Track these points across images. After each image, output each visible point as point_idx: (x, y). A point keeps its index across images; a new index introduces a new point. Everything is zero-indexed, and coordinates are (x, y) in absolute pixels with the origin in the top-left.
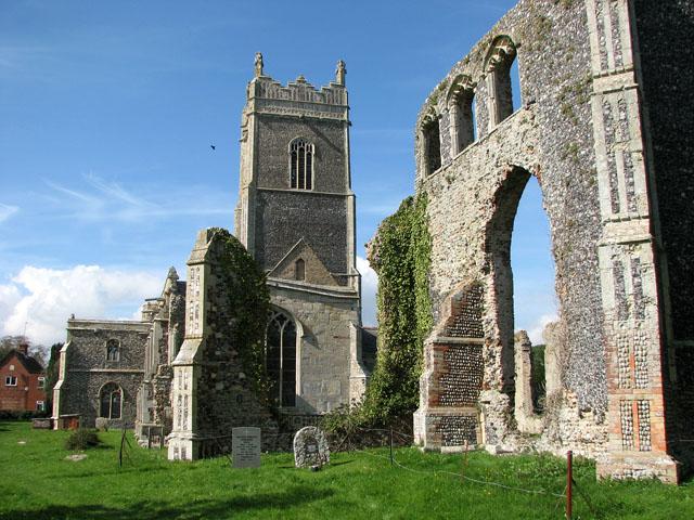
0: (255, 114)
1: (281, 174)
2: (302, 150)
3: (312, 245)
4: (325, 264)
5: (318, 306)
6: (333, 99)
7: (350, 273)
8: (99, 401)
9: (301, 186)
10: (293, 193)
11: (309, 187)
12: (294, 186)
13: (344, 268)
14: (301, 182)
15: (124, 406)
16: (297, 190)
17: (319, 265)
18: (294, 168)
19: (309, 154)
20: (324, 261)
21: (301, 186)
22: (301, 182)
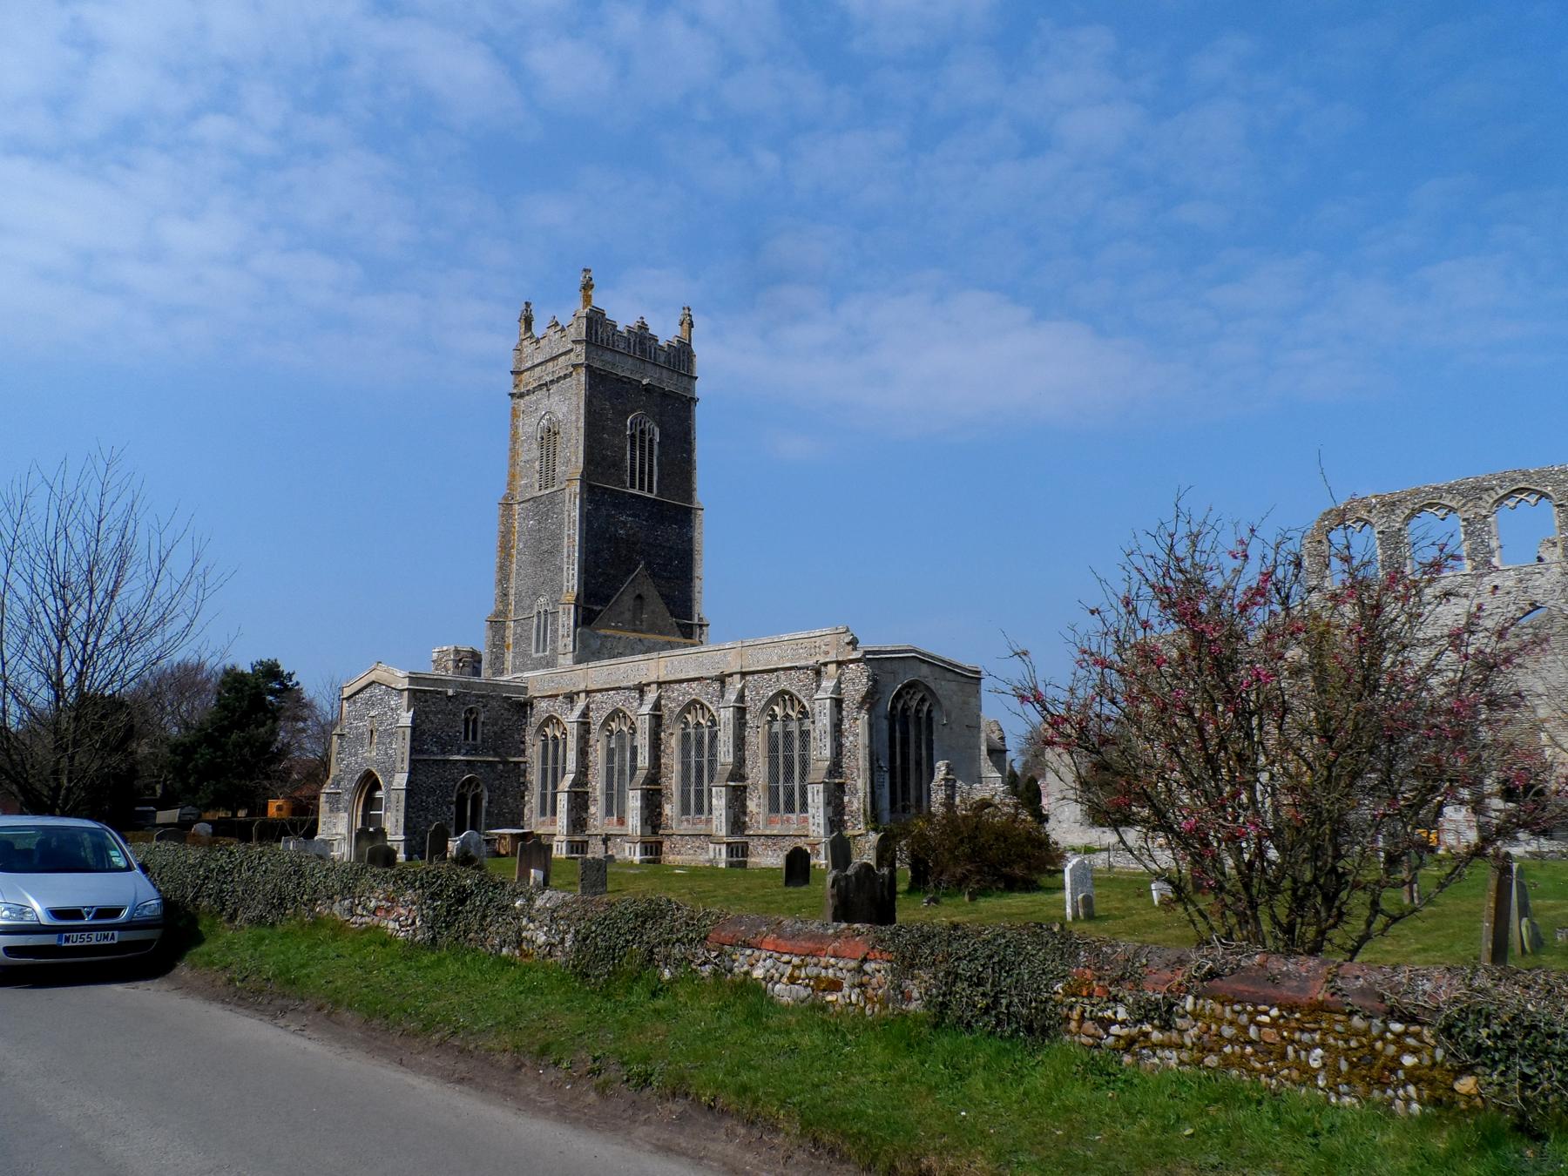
0: (588, 367)
2: (642, 432)
3: (653, 575)
5: (953, 686)
6: (681, 358)
7: (696, 621)
8: (453, 808)
9: (641, 488)
11: (650, 491)
12: (633, 486)
13: (688, 613)
14: (642, 480)
15: (488, 812)
16: (636, 491)
17: (660, 607)
18: (633, 458)
19: (651, 441)
20: (668, 600)
21: (641, 488)
22: (642, 480)
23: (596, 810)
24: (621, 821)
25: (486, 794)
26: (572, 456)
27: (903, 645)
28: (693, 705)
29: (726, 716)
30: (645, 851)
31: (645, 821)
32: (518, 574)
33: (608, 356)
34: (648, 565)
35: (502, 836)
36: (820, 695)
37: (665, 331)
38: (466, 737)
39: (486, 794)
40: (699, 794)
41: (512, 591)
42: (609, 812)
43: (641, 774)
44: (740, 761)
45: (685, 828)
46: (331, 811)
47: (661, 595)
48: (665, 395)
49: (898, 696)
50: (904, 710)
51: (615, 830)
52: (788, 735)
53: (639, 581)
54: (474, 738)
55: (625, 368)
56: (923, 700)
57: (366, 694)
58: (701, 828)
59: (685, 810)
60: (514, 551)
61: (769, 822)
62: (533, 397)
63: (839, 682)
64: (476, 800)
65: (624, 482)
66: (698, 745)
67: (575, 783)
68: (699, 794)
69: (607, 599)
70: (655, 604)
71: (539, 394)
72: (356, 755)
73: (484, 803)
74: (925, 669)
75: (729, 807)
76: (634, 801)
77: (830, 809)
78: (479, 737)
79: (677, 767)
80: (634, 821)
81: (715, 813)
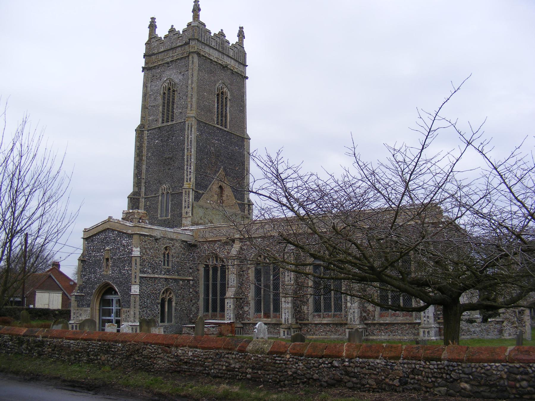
4: (233, 191)
7: (246, 202)
8: (159, 306)
10: (221, 129)
14: (222, 120)
15: (176, 309)
18: (218, 108)
25: (174, 298)
32: (147, 170)
33: (207, 49)
34: (225, 169)
37: (232, 39)
38: (164, 265)
39: (174, 298)
41: (143, 181)
45: (317, 321)
46: (78, 306)
48: (233, 72)
54: (168, 265)
55: (215, 55)
57: (102, 236)
59: (317, 309)
60: (144, 158)
61: (381, 316)
64: (170, 301)
65: (214, 121)
67: (237, 293)
72: (95, 272)
73: (174, 304)
78: (170, 264)
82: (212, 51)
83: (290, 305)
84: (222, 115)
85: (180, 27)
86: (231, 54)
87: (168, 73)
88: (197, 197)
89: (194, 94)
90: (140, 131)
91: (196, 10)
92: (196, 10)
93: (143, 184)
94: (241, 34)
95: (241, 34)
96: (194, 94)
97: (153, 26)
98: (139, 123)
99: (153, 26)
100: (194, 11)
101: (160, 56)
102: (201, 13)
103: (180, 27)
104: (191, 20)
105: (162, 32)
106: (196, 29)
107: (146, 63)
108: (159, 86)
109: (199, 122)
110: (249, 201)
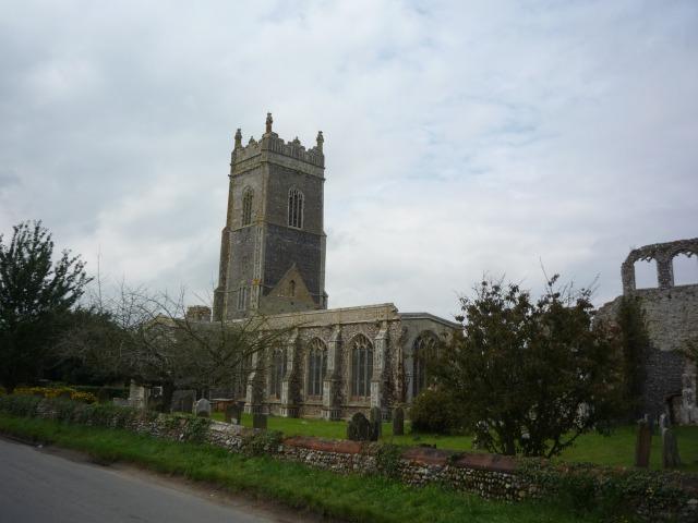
1: (283, 214)
3: (300, 270)
14: (295, 222)
18: (291, 211)
20: (307, 283)
22: (295, 222)
23: (267, 391)
24: (279, 397)
26: (260, 207)
27: (423, 311)
28: (316, 340)
29: (332, 346)
30: (290, 412)
31: (290, 398)
33: (279, 157)
34: (297, 266)
35: (219, 402)
36: (378, 337)
37: (309, 144)
40: (317, 385)
42: (272, 393)
43: (288, 374)
44: (339, 368)
45: (310, 402)
47: (304, 281)
48: (308, 176)
49: (419, 338)
50: (423, 345)
51: (276, 401)
52: (319, 358)
53: (293, 274)
55: (288, 163)
56: (432, 340)
58: (318, 402)
62: (241, 178)
63: (388, 331)
66: (318, 361)
68: (317, 385)
69: (275, 283)
70: (301, 287)
71: (245, 176)
74: (434, 325)
75: (332, 392)
76: (285, 387)
77: (381, 395)
79: (306, 371)
80: (285, 397)
81: (325, 394)
82: (284, 158)
83: (287, 389)
84: (295, 219)
85: (258, 138)
86: (307, 158)
87: (247, 180)
88: (266, 292)
89: (280, 198)
90: (226, 233)
91: (269, 122)
92: (269, 122)
93: (227, 281)
94: (320, 139)
95: (320, 139)
96: (280, 198)
97: (238, 138)
98: (225, 225)
99: (238, 138)
100: (267, 123)
101: (243, 165)
102: (273, 125)
103: (258, 138)
104: (265, 131)
105: (245, 143)
106: (271, 139)
107: (232, 171)
108: (238, 193)
109: (270, 225)
110: (324, 293)
